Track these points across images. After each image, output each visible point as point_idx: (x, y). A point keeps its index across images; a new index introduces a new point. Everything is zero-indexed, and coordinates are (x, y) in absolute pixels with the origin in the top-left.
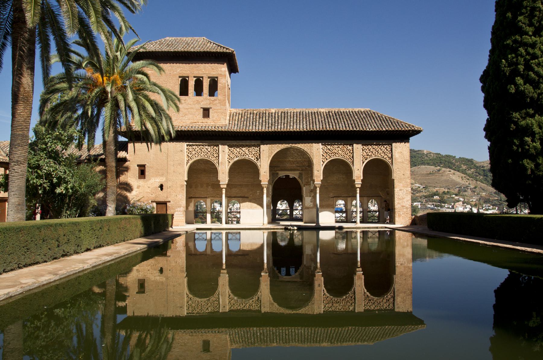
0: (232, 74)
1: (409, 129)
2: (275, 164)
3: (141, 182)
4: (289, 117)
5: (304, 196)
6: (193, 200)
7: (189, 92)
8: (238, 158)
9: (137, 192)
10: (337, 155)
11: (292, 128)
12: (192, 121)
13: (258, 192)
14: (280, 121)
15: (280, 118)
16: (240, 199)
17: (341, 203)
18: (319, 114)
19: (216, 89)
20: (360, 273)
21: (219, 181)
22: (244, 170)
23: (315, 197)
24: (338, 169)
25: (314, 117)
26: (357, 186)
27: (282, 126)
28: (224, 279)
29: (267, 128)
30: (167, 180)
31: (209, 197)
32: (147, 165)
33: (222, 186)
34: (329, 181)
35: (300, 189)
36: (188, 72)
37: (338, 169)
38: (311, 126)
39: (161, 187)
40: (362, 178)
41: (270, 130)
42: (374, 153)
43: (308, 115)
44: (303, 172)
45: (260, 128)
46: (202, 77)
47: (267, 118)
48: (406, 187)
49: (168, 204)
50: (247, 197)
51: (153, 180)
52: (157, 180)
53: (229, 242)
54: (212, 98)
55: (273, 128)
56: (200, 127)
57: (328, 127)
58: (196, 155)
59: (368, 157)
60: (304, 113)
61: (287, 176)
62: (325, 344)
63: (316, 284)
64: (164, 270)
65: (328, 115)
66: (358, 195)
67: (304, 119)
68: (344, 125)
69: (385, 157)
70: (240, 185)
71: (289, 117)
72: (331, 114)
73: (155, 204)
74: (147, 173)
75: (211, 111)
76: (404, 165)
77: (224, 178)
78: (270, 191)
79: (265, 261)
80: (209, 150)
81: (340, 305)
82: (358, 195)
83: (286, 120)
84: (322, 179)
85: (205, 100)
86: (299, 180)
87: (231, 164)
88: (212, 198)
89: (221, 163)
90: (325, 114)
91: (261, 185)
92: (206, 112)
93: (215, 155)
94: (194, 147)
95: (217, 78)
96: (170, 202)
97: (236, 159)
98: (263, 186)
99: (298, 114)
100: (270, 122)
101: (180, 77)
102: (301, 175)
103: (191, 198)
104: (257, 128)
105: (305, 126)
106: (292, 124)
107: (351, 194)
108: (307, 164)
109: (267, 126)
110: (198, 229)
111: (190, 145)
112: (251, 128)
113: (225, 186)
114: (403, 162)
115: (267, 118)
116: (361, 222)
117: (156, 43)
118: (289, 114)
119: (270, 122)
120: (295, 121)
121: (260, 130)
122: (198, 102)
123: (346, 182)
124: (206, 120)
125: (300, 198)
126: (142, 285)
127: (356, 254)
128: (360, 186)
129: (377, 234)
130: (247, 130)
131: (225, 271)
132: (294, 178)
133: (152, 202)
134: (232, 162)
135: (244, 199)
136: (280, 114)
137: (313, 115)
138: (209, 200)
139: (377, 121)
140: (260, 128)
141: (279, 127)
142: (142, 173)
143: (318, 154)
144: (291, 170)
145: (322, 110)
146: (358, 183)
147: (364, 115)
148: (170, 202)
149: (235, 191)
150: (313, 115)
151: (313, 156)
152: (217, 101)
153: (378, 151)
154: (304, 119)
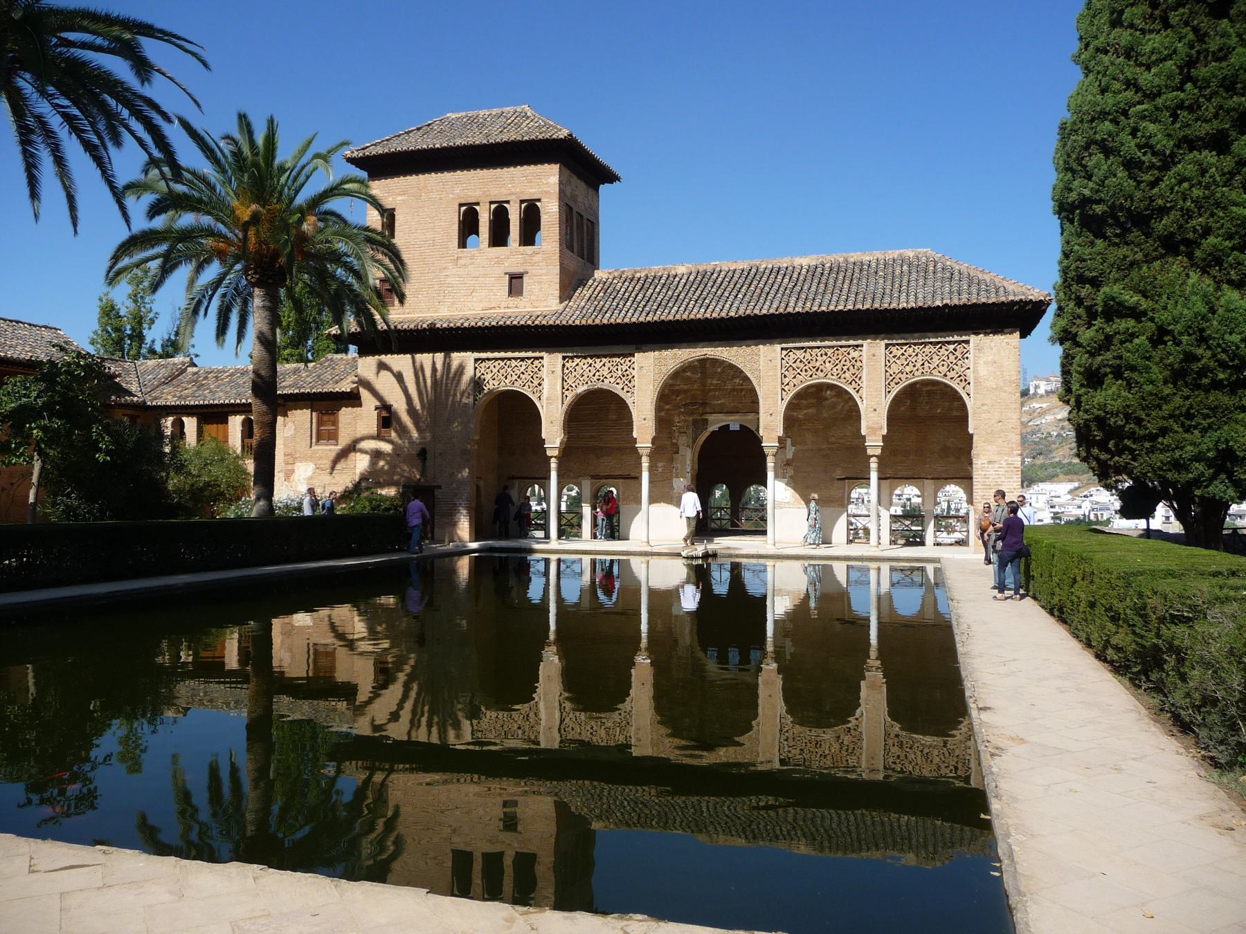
0: (604, 189)
1: (1011, 298)
2: (670, 396)
6: (517, 482)
8: (585, 387)
10: (822, 375)
12: (486, 305)
13: (660, 465)
18: (788, 272)
19: (537, 227)
22: (597, 414)
26: (870, 452)
28: (551, 663)
33: (549, 453)
34: (832, 440)
36: (478, 193)
40: (885, 432)
42: (918, 365)
46: (508, 202)
48: (1009, 455)
49: (437, 492)
54: (529, 249)
58: (496, 383)
59: (903, 377)
60: (754, 270)
62: (910, 859)
63: (762, 692)
66: (874, 476)
69: (950, 375)
70: (620, 449)
72: (819, 270)
76: (1003, 395)
77: (553, 435)
78: (688, 462)
80: (522, 369)
81: (597, 730)
82: (874, 476)
83: (699, 292)
84: (781, 433)
85: (513, 254)
87: (567, 402)
90: (804, 271)
92: (515, 282)
93: (536, 382)
95: (539, 200)
96: (440, 487)
97: (581, 389)
98: (640, 451)
101: (461, 205)
103: (513, 478)
108: (747, 398)
110: (492, 549)
111: (483, 360)
112: (608, 315)
113: (556, 453)
114: (998, 389)
117: (418, 129)
122: (499, 261)
124: (513, 301)
128: (878, 452)
131: (554, 649)
134: (570, 396)
139: (930, 282)
143: (772, 373)
145: (798, 261)
146: (874, 444)
147: (905, 268)
148: (440, 487)
151: (759, 377)
153: (924, 360)
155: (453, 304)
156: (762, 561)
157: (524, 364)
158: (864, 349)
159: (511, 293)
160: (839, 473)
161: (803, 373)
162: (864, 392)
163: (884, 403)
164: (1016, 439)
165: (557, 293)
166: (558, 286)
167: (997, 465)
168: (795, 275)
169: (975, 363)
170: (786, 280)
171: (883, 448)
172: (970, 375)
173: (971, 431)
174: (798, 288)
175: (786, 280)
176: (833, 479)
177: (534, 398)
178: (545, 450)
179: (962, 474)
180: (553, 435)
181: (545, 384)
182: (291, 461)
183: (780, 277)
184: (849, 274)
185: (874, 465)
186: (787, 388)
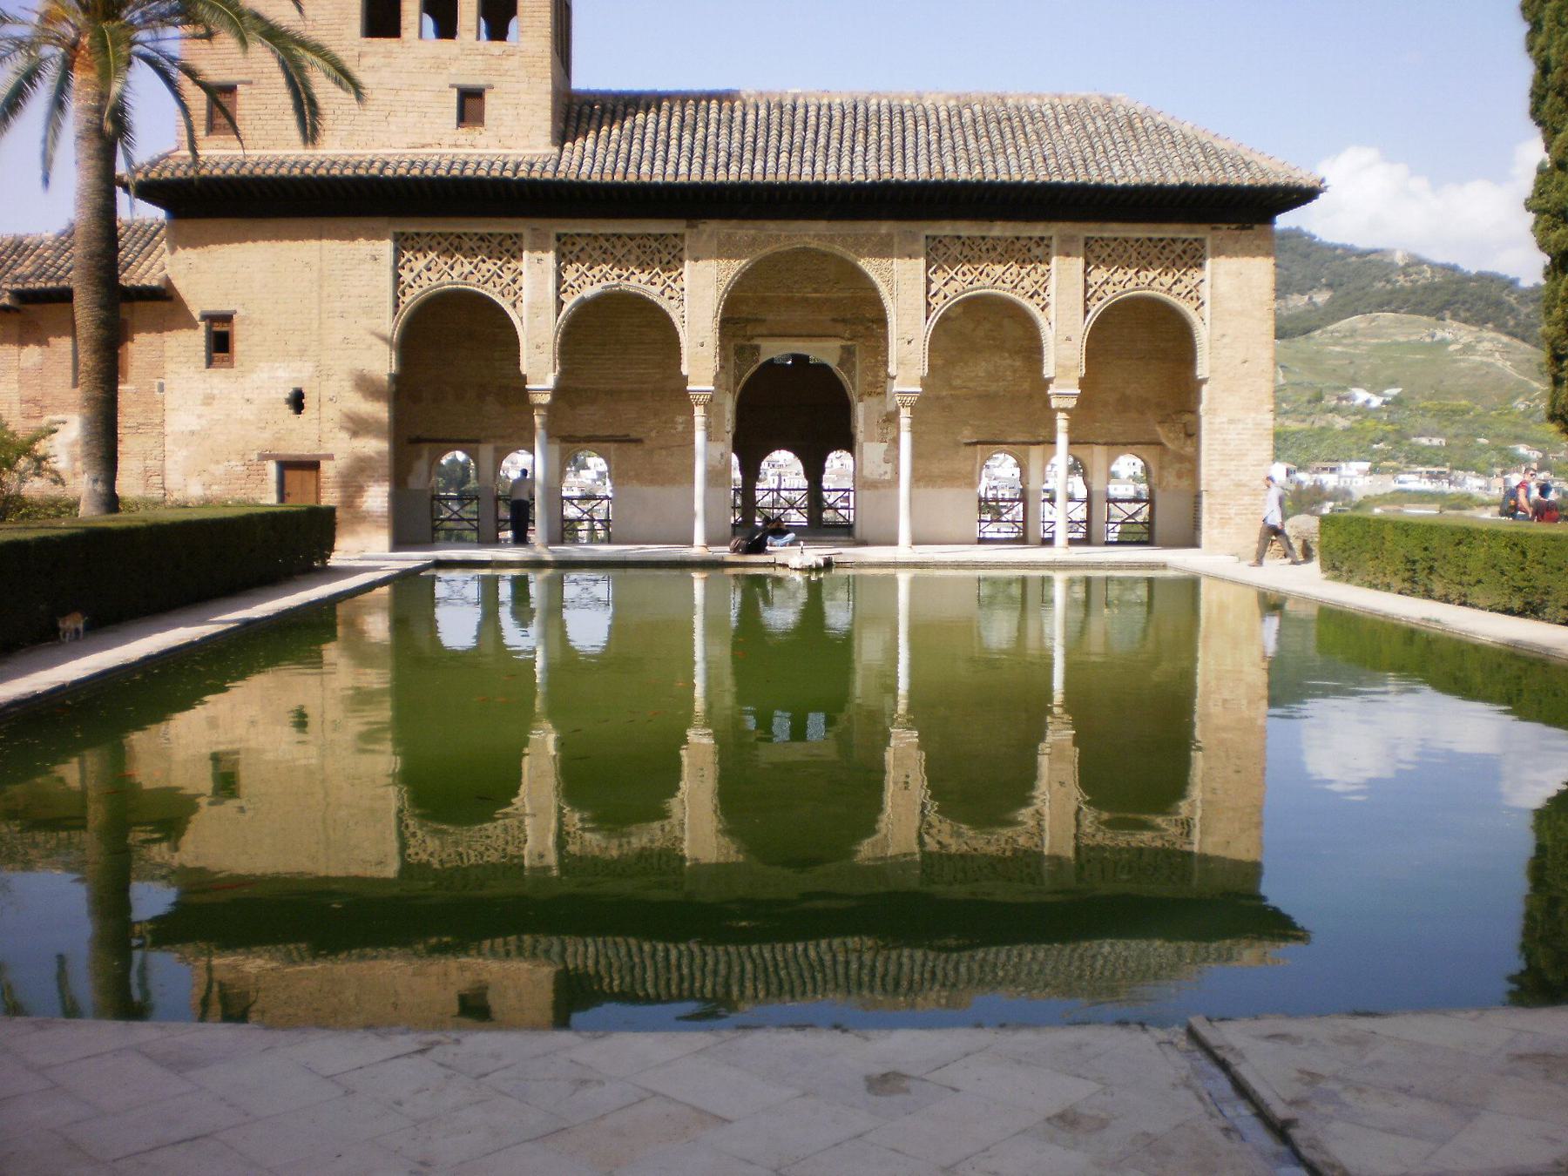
3: (218, 379)
4: (799, 126)
5: (860, 436)
6: (426, 449)
7: (404, 23)
9: (204, 422)
10: (988, 281)
11: (807, 169)
13: (680, 419)
14: (761, 143)
15: (762, 128)
16: (612, 447)
17: (1001, 471)
20: (1059, 735)
21: (524, 379)
23: (896, 442)
24: (989, 336)
25: (898, 127)
27: (771, 163)
29: (709, 169)
30: (322, 373)
31: (486, 440)
32: (241, 312)
34: (957, 382)
35: (843, 410)
37: (989, 336)
38: (885, 162)
39: (297, 401)
41: (721, 177)
43: (873, 120)
44: (858, 346)
45: (683, 169)
47: (712, 129)
49: (324, 465)
50: (638, 441)
51: (261, 377)
52: (280, 373)
53: (567, 614)
54: (496, 47)
55: (734, 168)
56: (445, 163)
57: (950, 167)
58: (434, 276)
59: (1109, 288)
60: (861, 109)
61: (800, 360)
63: (892, 777)
64: (314, 720)
65: (955, 120)
66: (1062, 439)
67: (860, 136)
68: (1013, 162)
70: (610, 393)
71: (799, 126)
72: (967, 114)
73: (272, 467)
74: (239, 346)
75: (489, 97)
79: (699, 692)
82: (1062, 439)
84: (922, 369)
85: (469, 54)
86: (843, 376)
88: (500, 444)
89: (531, 306)
90: (943, 115)
91: (686, 393)
92: (470, 104)
93: (508, 277)
94: (423, 242)
96: (330, 457)
97: (589, 291)
99: (837, 114)
100: (723, 144)
102: (848, 353)
103: (419, 440)
104: (670, 169)
105: (858, 163)
106: (808, 154)
107: (1043, 434)
108: (865, 318)
109: (710, 160)
112: (645, 168)
115: (712, 129)
116: (1072, 542)
118: (800, 112)
119: (723, 144)
120: (822, 141)
121: (683, 179)
122: (439, 65)
123: (1026, 386)
125: (848, 443)
126: (226, 781)
127: (1049, 666)
129: (1142, 592)
130: (632, 178)
132: (823, 368)
133: (264, 457)
134: (570, 302)
135: (625, 446)
136: (763, 113)
137: (897, 119)
138: (486, 451)
140: (683, 169)
141: (759, 165)
142: (220, 344)
144: (810, 336)
147: (1100, 122)
148: (330, 457)
149: (589, 417)
150: (897, 119)
152: (513, 62)
154: (860, 136)
155: (351, 134)
156: (890, 571)
157: (484, 245)
158: (1055, 242)
159: (462, 119)
160: (967, 434)
161: (960, 277)
162: (1051, 310)
163: (1080, 329)
164: (1266, 388)
165: (547, 126)
166: (548, 114)
167: (1241, 426)
168: (933, 120)
169: (1213, 275)
170: (922, 128)
171: (1083, 400)
172: (1205, 292)
173: (1202, 371)
174: (947, 143)
175: (922, 128)
176: (957, 444)
177: (505, 304)
178: (526, 393)
179: (1147, 438)
180: (539, 368)
181: (525, 281)
182: (35, 411)
183: (885, 122)
184: (1016, 122)
185: (1062, 422)
186: (933, 302)
